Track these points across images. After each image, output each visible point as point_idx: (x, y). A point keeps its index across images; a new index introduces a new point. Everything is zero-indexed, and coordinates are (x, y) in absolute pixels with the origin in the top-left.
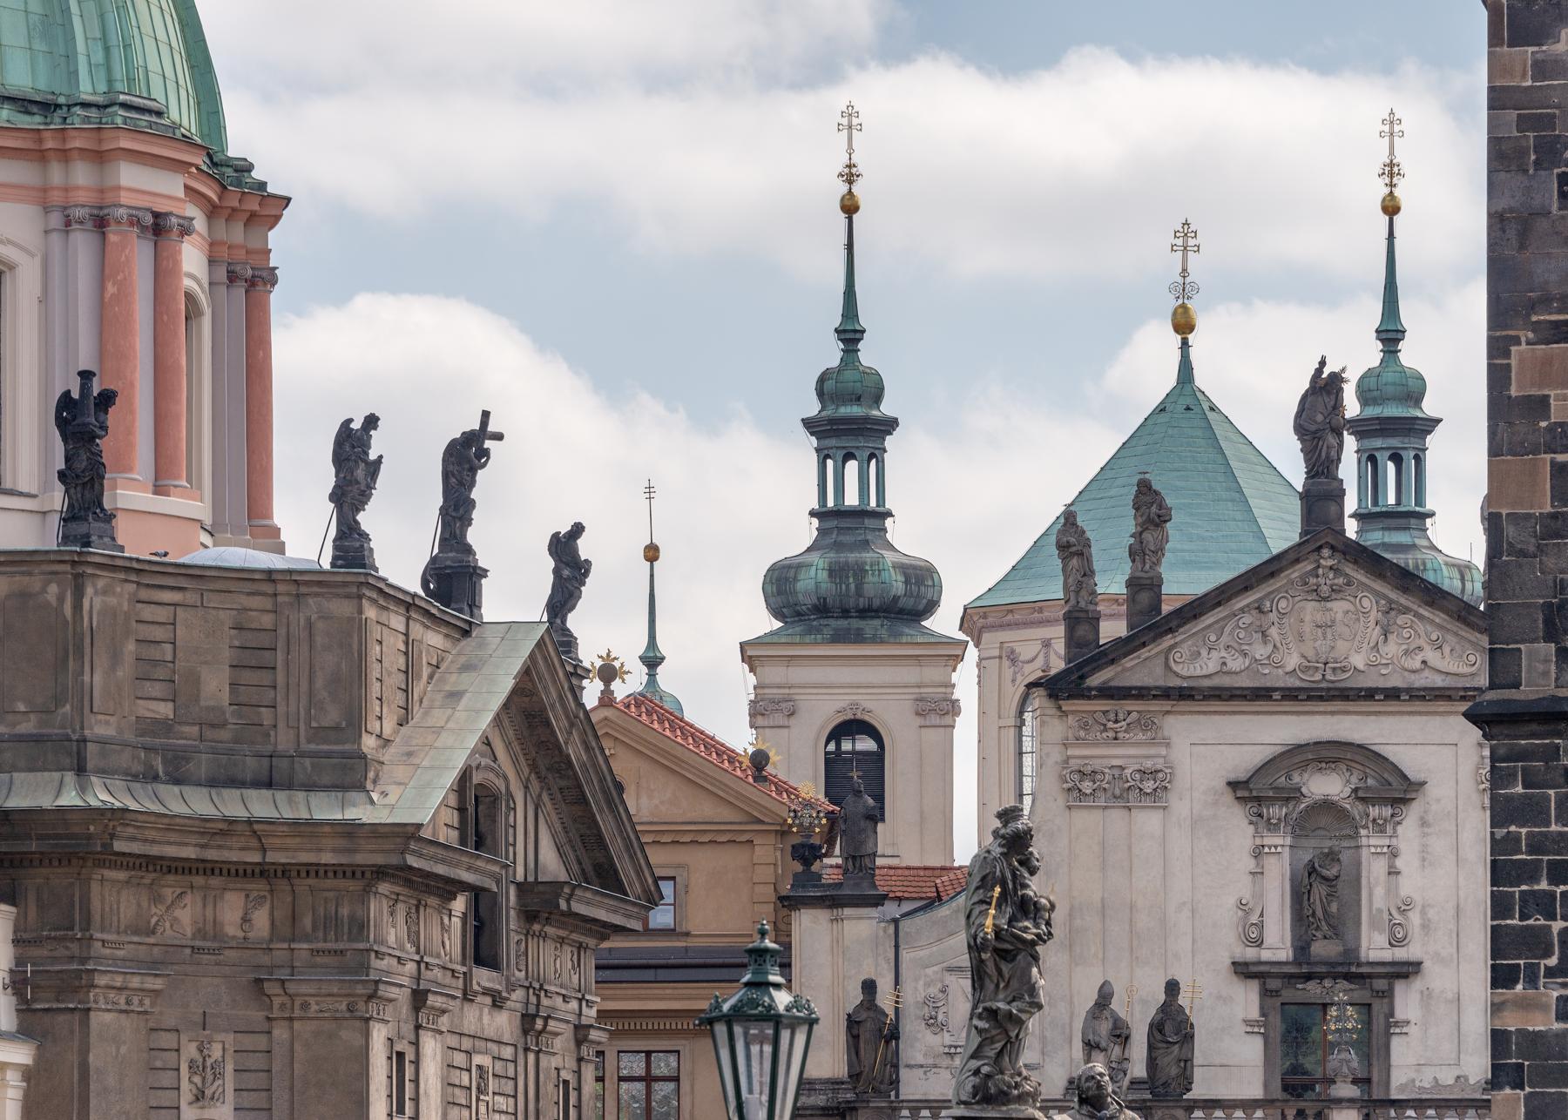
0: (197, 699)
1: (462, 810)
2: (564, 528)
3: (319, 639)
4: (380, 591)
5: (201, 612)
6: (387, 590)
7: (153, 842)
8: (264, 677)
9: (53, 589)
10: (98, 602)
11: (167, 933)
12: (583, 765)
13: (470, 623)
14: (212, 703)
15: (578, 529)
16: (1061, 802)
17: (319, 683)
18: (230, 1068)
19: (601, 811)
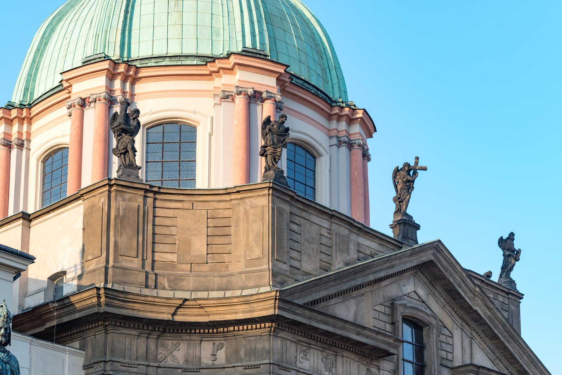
0: (189, 253)
3: (251, 218)
4: (292, 197)
5: (191, 211)
6: (296, 197)
9: (103, 200)
12: (489, 318)
13: (402, 243)
14: (197, 254)
17: (251, 238)
19: (509, 342)
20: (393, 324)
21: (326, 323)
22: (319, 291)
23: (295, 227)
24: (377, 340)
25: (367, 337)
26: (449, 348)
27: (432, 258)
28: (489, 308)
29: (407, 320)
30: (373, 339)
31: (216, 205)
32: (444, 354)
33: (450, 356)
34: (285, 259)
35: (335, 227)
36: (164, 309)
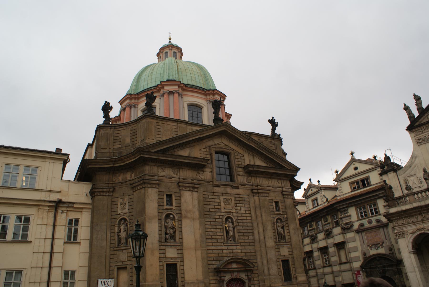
1: (211, 155)
2: (271, 119)
4: (157, 117)
7: (102, 165)
8: (135, 136)
10: (103, 132)
11: (117, 181)
12: (258, 147)
15: (273, 118)
16: (417, 145)
18: (127, 202)
20: (211, 155)
21: (167, 157)
22: (163, 146)
23: (159, 127)
24: (195, 161)
25: (189, 160)
26: (242, 161)
27: (225, 129)
28: (256, 143)
29: (216, 152)
30: (193, 160)
31: (133, 126)
32: (240, 163)
33: (243, 164)
34: (153, 138)
35: (179, 125)
36: (111, 163)
